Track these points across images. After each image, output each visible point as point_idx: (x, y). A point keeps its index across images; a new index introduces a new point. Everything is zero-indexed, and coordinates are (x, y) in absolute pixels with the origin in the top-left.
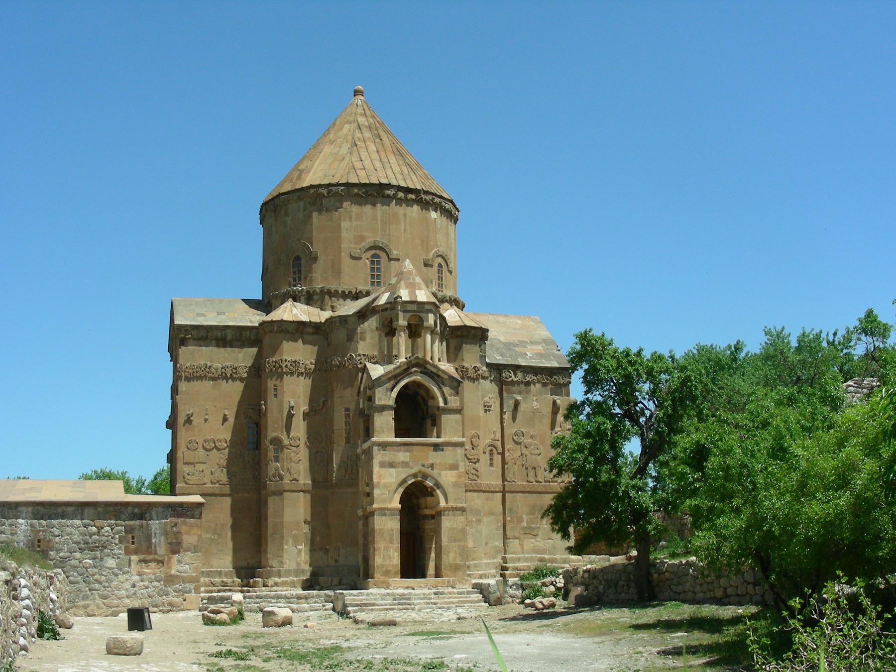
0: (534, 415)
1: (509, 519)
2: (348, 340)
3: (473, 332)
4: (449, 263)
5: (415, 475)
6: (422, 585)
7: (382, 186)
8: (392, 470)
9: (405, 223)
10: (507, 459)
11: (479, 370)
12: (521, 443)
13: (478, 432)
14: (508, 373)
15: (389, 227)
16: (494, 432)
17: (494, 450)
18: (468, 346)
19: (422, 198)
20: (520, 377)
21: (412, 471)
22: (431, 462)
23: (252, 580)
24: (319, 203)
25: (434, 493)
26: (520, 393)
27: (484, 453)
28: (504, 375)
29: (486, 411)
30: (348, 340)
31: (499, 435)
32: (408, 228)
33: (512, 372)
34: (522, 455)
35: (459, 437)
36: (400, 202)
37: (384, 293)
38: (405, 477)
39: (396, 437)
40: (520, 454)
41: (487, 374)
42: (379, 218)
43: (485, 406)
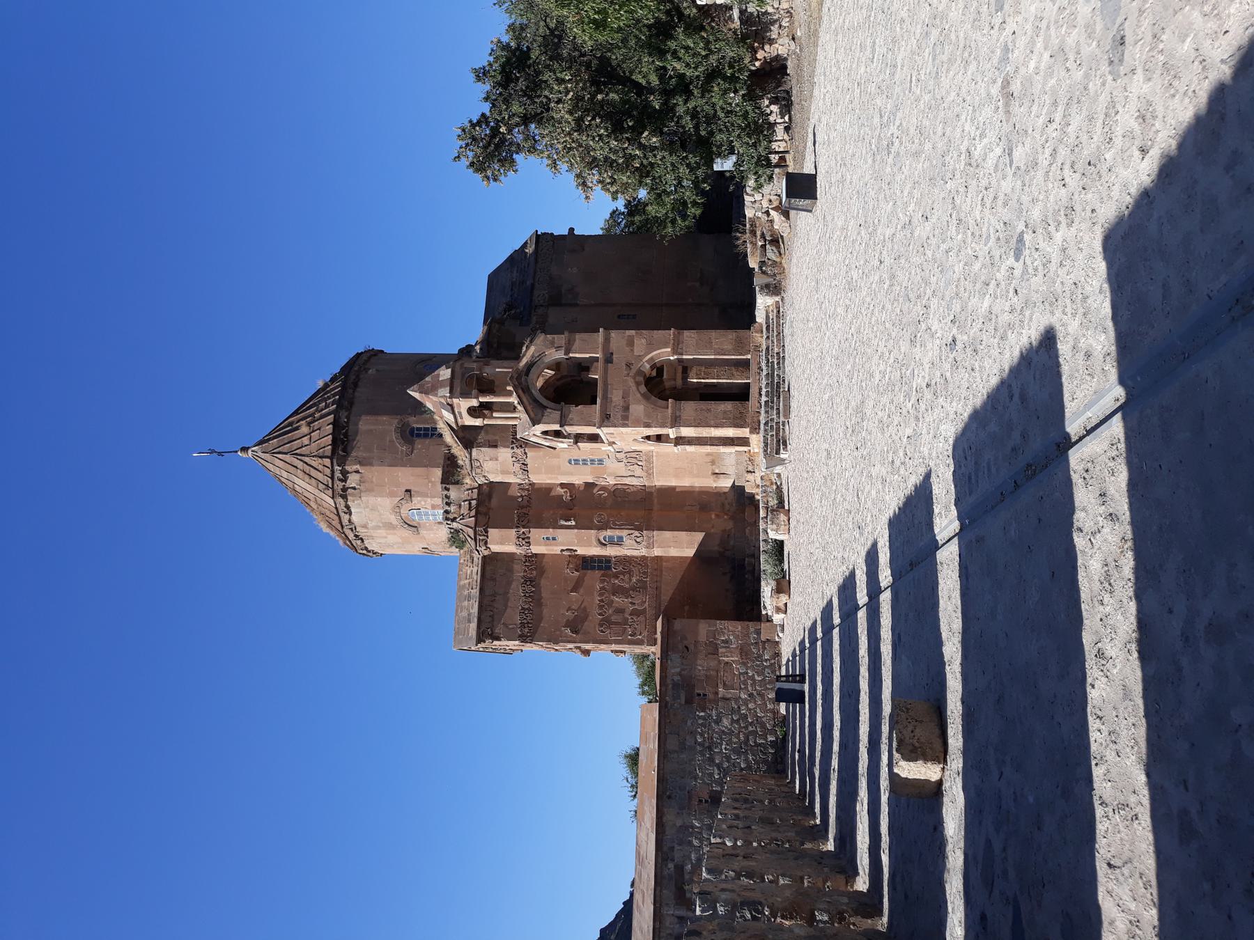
1: (690, 300)
2: (497, 460)
5: (638, 384)
6: (757, 378)
8: (632, 408)
21: (634, 388)
22: (624, 364)
23: (747, 568)
24: (353, 491)
25: (658, 366)
30: (497, 460)
35: (599, 337)
37: (442, 417)
38: (639, 395)
39: (596, 404)
42: (372, 427)
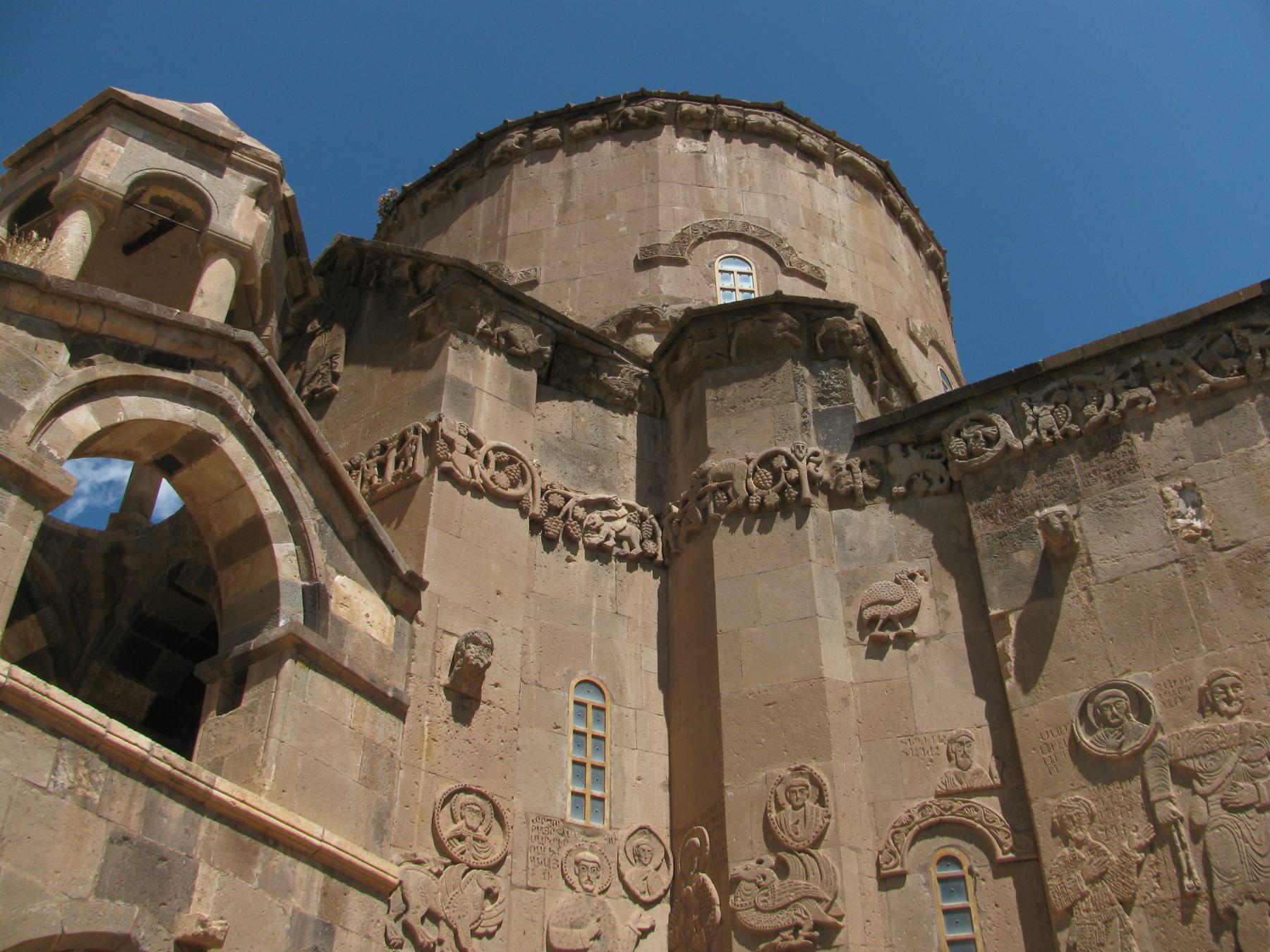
0: (1191, 573)
3: (744, 329)
4: (782, 254)
7: (482, 143)
9: (569, 191)
10: (1059, 888)
11: (791, 464)
12: (1137, 755)
13: (813, 766)
14: (979, 430)
15: (507, 219)
16: (957, 749)
17: (971, 856)
18: (732, 392)
19: (625, 116)
20: (1047, 419)
26: (1072, 495)
27: (890, 881)
28: (956, 445)
29: (877, 649)
31: (983, 761)
32: (576, 198)
33: (996, 418)
34: (1162, 836)
36: (546, 151)
40: (1141, 833)
41: (863, 478)
43: (866, 625)
